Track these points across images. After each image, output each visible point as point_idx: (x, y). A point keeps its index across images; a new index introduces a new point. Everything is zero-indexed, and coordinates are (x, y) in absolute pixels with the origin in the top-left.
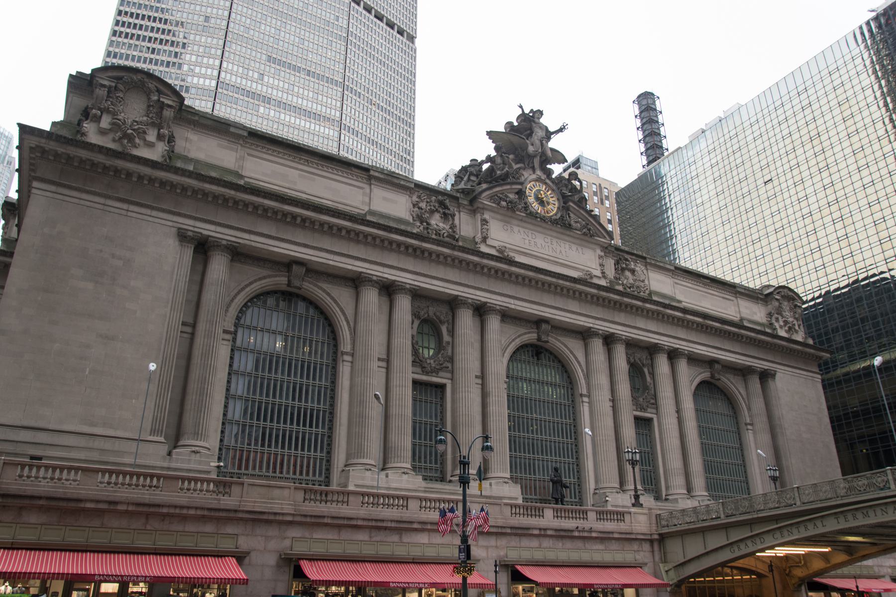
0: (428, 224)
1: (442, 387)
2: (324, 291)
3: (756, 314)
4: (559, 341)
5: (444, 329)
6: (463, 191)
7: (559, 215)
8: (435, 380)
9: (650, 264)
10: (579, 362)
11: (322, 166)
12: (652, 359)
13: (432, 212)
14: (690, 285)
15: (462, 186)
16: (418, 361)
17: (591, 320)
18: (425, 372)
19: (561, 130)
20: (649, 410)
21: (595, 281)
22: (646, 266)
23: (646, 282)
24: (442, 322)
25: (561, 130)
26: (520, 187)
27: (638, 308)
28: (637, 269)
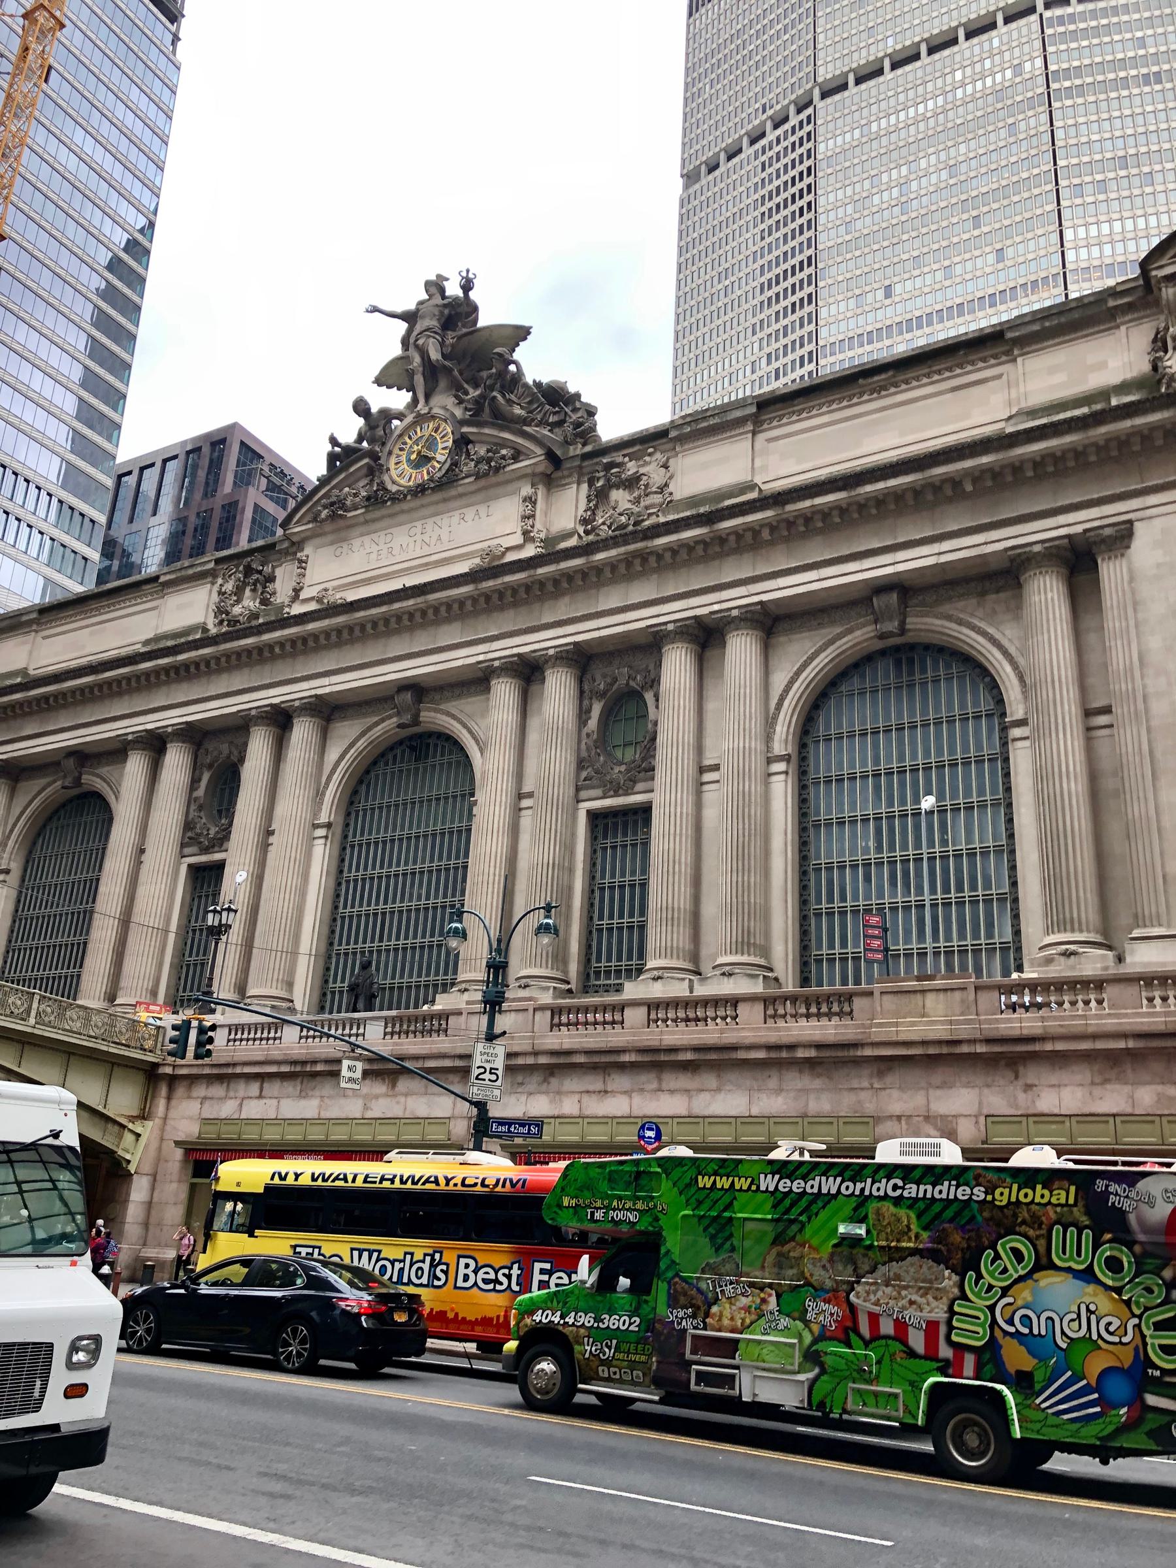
0: (227, 613)
3: (1103, 365)
7: (447, 466)
8: (218, 856)
14: (825, 419)
19: (467, 286)
20: (640, 786)
21: (511, 557)
23: (671, 488)
25: (467, 286)
27: (583, 573)
28: (642, 470)
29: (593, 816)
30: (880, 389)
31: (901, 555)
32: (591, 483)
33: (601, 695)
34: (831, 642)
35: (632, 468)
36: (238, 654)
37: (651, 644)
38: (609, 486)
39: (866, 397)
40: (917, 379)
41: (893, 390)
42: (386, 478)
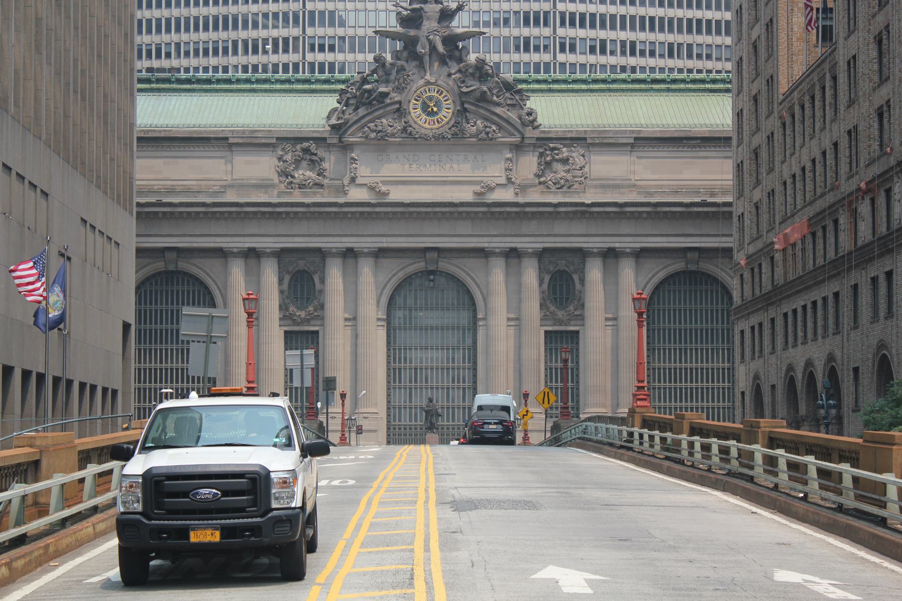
0: (293, 177)
1: (317, 332)
2: (197, 266)
4: (452, 264)
5: (316, 278)
6: (333, 127)
7: (452, 122)
9: (593, 145)
10: (477, 284)
11: (184, 147)
12: (584, 263)
13: (297, 162)
15: (333, 121)
16: (286, 316)
17: (486, 239)
18: (295, 323)
19: (460, 8)
20: (573, 322)
22: (588, 147)
23: (586, 169)
24: (315, 272)
26: (397, 106)
29: (546, 332)
30: (694, 147)
31: (704, 239)
32: (541, 155)
33: (548, 272)
34: (666, 267)
35: (565, 152)
36: (321, 213)
37: (582, 254)
38: (554, 160)
39: (685, 149)
40: (710, 147)
41: (698, 149)
42: (409, 118)
